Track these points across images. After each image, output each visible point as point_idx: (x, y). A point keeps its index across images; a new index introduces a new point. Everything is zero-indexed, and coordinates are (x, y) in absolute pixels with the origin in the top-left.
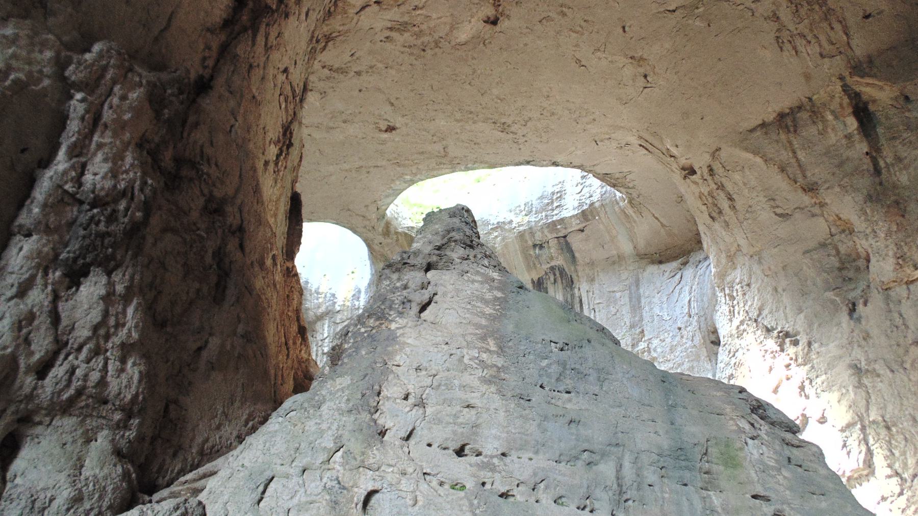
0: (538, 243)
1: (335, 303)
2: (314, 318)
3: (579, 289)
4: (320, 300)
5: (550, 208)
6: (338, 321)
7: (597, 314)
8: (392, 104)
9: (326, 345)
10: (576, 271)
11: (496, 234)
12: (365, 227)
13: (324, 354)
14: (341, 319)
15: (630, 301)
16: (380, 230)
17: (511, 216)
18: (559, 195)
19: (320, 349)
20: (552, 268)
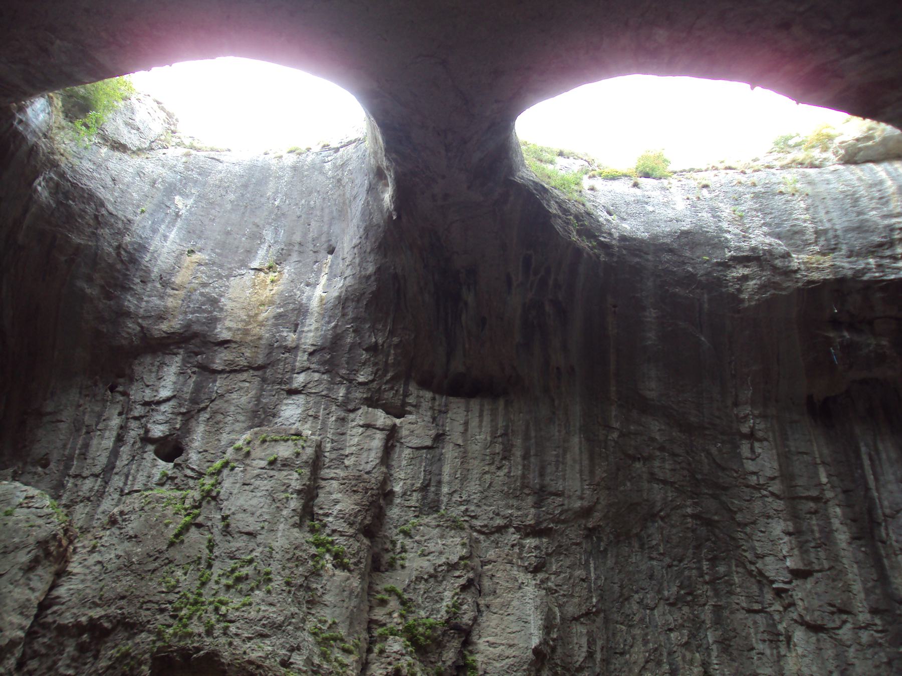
1: (213, 321)
2: (136, 341)
5: (888, 253)
6: (218, 365)
11: (746, 271)
13: (146, 439)
14: (231, 363)
17: (781, 246)
19: (133, 424)
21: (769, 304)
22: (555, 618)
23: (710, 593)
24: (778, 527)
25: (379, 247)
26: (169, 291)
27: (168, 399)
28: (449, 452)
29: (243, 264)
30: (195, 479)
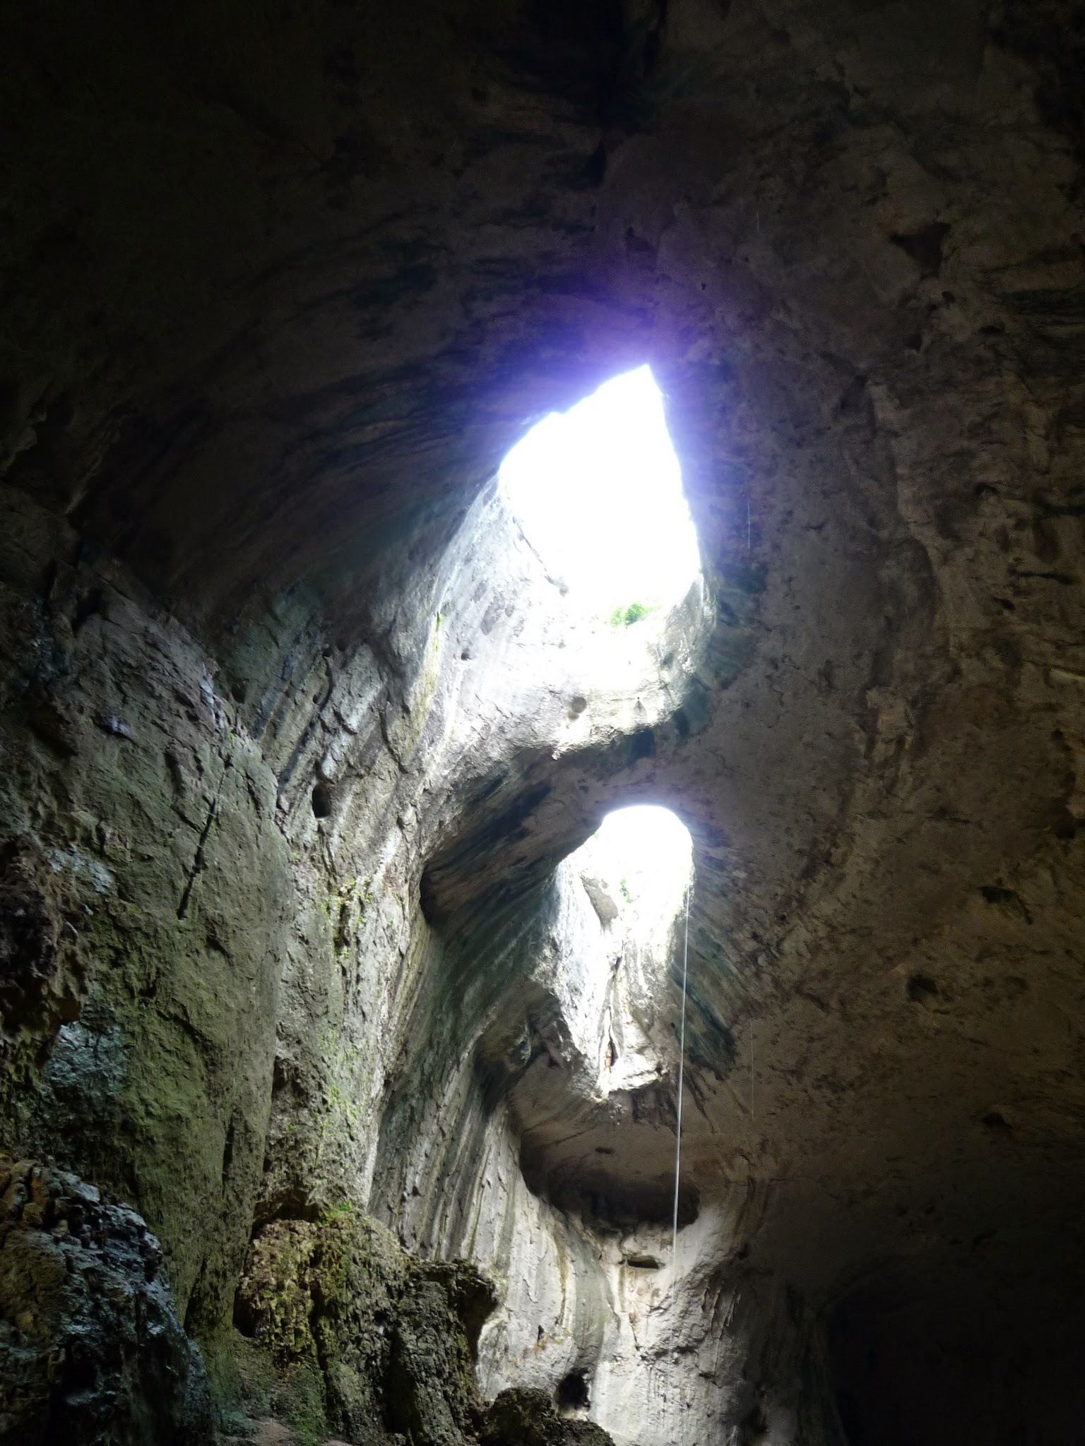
8: (972, 1040)
19: (319, 731)
21: (536, 985)
25: (517, 748)
27: (351, 732)
30: (327, 870)
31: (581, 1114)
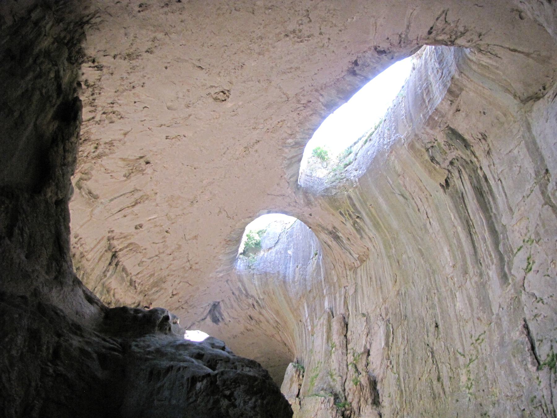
0: (429, 145)
3: (481, 168)
4: (297, 287)
5: (424, 107)
7: (503, 183)
9: (309, 324)
10: (473, 153)
12: (289, 205)
15: (528, 150)
16: (302, 202)
18: (427, 90)
20: (451, 163)
22: (390, 333)
23: (436, 291)
24: (446, 250)
26: (296, 284)
28: (360, 291)
29: (309, 259)
31: (489, 61)
